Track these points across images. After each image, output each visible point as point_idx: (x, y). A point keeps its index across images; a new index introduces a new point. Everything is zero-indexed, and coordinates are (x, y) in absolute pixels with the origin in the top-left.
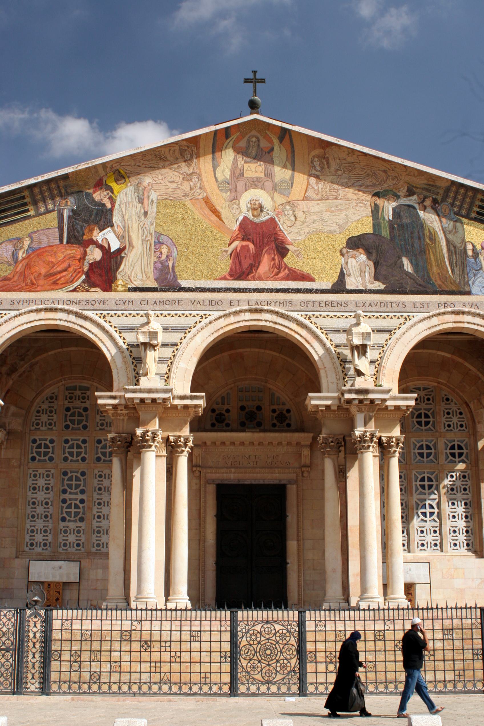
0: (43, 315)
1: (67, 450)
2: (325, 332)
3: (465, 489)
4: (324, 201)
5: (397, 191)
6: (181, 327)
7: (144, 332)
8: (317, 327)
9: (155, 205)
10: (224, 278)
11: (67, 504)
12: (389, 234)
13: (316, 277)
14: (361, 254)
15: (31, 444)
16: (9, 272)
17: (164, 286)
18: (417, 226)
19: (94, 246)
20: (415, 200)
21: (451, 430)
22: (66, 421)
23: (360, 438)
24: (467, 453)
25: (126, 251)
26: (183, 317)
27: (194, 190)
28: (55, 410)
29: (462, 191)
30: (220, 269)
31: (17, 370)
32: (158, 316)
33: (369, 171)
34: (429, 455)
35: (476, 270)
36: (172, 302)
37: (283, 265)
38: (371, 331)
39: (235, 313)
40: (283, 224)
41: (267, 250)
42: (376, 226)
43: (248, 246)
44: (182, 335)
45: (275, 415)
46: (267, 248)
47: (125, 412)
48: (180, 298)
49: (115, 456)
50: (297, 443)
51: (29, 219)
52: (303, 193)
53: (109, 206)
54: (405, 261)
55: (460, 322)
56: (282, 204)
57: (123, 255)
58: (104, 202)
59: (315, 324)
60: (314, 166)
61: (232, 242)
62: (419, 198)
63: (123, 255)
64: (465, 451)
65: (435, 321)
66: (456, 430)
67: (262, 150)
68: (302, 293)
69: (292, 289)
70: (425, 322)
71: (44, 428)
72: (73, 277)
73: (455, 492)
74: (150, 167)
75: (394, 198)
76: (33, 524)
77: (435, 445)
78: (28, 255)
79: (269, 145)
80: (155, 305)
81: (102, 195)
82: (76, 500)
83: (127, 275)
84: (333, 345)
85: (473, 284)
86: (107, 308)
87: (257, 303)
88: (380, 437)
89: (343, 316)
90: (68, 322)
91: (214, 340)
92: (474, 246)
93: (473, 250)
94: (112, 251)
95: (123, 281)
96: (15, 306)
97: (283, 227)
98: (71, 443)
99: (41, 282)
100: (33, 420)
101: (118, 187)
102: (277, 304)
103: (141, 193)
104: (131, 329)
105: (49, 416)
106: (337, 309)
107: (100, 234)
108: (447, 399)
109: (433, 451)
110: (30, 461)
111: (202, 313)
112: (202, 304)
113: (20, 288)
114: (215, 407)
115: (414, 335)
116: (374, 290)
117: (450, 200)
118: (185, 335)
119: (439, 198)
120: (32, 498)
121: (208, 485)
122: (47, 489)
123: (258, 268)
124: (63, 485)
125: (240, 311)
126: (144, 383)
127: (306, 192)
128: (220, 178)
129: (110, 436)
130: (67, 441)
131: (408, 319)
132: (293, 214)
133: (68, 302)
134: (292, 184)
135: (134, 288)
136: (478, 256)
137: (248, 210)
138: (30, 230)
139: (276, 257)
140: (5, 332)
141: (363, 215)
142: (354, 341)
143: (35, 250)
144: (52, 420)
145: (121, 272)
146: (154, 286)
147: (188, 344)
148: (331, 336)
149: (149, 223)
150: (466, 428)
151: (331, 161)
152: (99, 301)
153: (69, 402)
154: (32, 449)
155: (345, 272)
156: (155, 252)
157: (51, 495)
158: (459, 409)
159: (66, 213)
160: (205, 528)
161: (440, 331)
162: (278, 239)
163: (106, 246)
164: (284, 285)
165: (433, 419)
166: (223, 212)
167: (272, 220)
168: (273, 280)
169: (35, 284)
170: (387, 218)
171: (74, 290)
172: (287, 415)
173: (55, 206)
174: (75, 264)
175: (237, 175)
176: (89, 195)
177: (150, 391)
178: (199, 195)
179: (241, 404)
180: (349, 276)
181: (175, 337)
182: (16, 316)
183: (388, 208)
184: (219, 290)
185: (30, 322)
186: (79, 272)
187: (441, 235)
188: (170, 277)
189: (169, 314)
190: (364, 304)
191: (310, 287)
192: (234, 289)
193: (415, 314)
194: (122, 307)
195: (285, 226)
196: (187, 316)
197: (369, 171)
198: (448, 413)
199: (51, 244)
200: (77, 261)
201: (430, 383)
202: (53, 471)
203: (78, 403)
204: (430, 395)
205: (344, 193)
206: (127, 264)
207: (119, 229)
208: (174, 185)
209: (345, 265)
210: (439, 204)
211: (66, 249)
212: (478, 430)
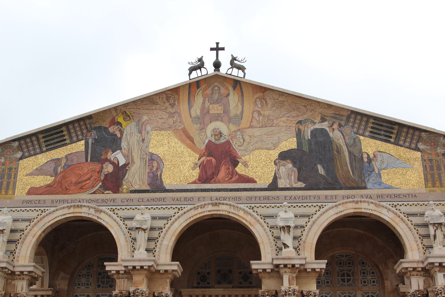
0: (72, 210)
4: (263, 128)
5: (314, 119)
6: (165, 216)
8: (258, 215)
10: (194, 182)
12: (308, 149)
17: (153, 189)
18: (328, 143)
19: (108, 162)
20: (326, 125)
21: (366, 285)
22: (98, 282)
23: (285, 292)
25: (129, 166)
26: (166, 210)
27: (176, 124)
28: (91, 275)
29: (359, 117)
33: (294, 107)
35: (370, 172)
36: (159, 199)
37: (235, 172)
39: (202, 207)
40: (235, 145)
41: (224, 162)
42: (299, 143)
43: (211, 160)
44: (165, 221)
45: (241, 276)
46: (224, 161)
48: (165, 196)
51: (66, 146)
53: (119, 135)
54: (320, 167)
55: (359, 208)
56: (235, 131)
57: (127, 168)
59: (257, 212)
60: (257, 105)
61: (201, 158)
62: (329, 123)
63: (127, 168)
65: (341, 208)
66: (370, 285)
67: (222, 95)
68: (248, 191)
70: (334, 209)
71: (83, 288)
72: (93, 184)
74: (147, 109)
75: (311, 124)
79: (227, 92)
81: (115, 128)
83: (130, 181)
84: (269, 227)
85: (368, 181)
87: (217, 199)
91: (187, 225)
92: (368, 155)
94: (120, 165)
95: (127, 186)
97: (235, 146)
99: (72, 188)
102: (231, 199)
103: (141, 127)
105: (87, 279)
106: (271, 201)
107: (113, 155)
108: (363, 263)
111: (179, 206)
112: (179, 200)
113: (58, 192)
117: (351, 124)
118: (167, 222)
119: (343, 123)
123: (218, 175)
127: (251, 122)
128: (193, 114)
131: (322, 208)
132: (242, 137)
133: (90, 201)
134: (242, 117)
135: (134, 190)
136: (371, 162)
137: (212, 136)
139: (230, 167)
140: (46, 222)
141: (290, 137)
143: (69, 166)
144: (89, 281)
145: (126, 180)
147: (169, 228)
148: (267, 220)
149: (145, 146)
150: (377, 283)
151: (268, 101)
152: (111, 200)
153: (101, 269)
155: (278, 176)
156: (149, 166)
158: (372, 270)
159: (90, 141)
161: (345, 215)
162: (232, 155)
163: (116, 162)
164: (235, 186)
165: (353, 278)
166: (195, 137)
167: (228, 143)
168: (228, 183)
170: (306, 138)
173: (83, 136)
176: (106, 129)
177: (140, 260)
178: (179, 127)
180: (280, 178)
183: (308, 131)
185: (63, 215)
186: (98, 180)
187: (345, 148)
188: (158, 182)
189: (157, 208)
190: (291, 198)
192: (201, 189)
193: (326, 204)
194: (126, 204)
195: (237, 146)
196: (169, 209)
197: (294, 107)
198: (364, 273)
199: (79, 162)
200: (97, 173)
204: (351, 260)
205: (277, 122)
206: (130, 175)
208: (162, 121)
209: (277, 171)
211: (90, 165)
212: (386, 285)
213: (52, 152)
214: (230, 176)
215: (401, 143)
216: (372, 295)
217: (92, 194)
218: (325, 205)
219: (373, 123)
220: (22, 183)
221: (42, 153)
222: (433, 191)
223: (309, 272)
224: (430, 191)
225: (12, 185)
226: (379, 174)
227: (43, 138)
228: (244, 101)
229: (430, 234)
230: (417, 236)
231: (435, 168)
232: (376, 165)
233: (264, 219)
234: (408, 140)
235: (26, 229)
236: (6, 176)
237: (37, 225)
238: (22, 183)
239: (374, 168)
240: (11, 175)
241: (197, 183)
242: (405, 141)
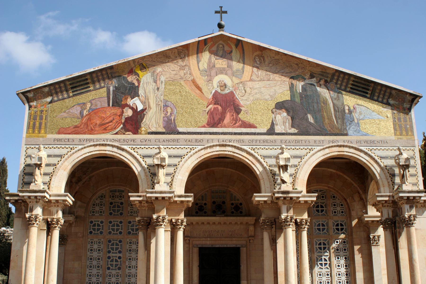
0: (98, 148)
1: (111, 227)
2: (263, 158)
3: (345, 250)
7: (157, 158)
8: (258, 155)
9: (163, 84)
10: (204, 127)
11: (110, 260)
13: (258, 126)
14: (284, 112)
15: (90, 224)
16: (78, 123)
17: (169, 131)
19: (128, 107)
20: (314, 81)
21: (336, 215)
23: (284, 219)
24: (346, 228)
25: (147, 111)
28: (104, 204)
30: (201, 121)
31: (81, 180)
32: (165, 149)
33: (288, 64)
34: (323, 229)
35: (351, 121)
36: (174, 140)
38: (290, 157)
39: (211, 147)
40: (238, 95)
42: (293, 95)
43: (217, 108)
44: (179, 159)
45: (233, 206)
46: (229, 109)
47: (146, 205)
49: (140, 231)
50: (246, 223)
52: (250, 77)
53: (136, 84)
54: (309, 116)
55: (342, 152)
56: (237, 83)
57: (145, 113)
58: (134, 82)
59: (257, 153)
61: (209, 106)
62: (317, 80)
63: (145, 113)
64: (344, 227)
65: (327, 151)
66: (339, 215)
67: (226, 52)
69: (244, 133)
70: (321, 152)
72: (115, 126)
73: (339, 251)
76: (91, 271)
77: (327, 224)
78: (89, 113)
79: (230, 49)
80: (164, 142)
81: (132, 78)
82: (116, 257)
83: (147, 124)
85: (349, 129)
86: (136, 144)
87: (223, 141)
88: (296, 219)
89: (273, 148)
90: (112, 152)
93: (349, 110)
94: (138, 110)
96: (82, 143)
98: (113, 223)
99: (97, 129)
100: (91, 210)
101: (142, 73)
102: (235, 141)
103: (155, 77)
104: (149, 156)
105: (100, 207)
107: (132, 101)
108: (334, 197)
109: (326, 227)
110: (89, 234)
111: (191, 147)
112: (191, 142)
113: (84, 132)
114: (198, 202)
115: (315, 159)
116: (291, 133)
117: (335, 81)
119: (329, 80)
120: (90, 256)
121: (194, 248)
122: (99, 250)
123: (223, 121)
124: (108, 248)
125: (213, 146)
126: (157, 188)
127: (251, 77)
128: (201, 68)
129: (137, 219)
130: (110, 222)
131: (311, 150)
133: (113, 141)
134: (243, 71)
136: (352, 113)
137: (218, 87)
138: (91, 98)
139: (234, 114)
140: (76, 158)
142: (280, 163)
145: (144, 123)
146: (163, 131)
148: (266, 160)
149: (160, 94)
150: (345, 213)
151: (266, 58)
152: (131, 140)
153: (112, 199)
154: (90, 227)
155: (274, 123)
156: (163, 111)
157: (101, 254)
158: (341, 202)
159: (111, 89)
160: (192, 273)
161: (330, 157)
163: (135, 108)
164: (239, 130)
167: (232, 93)
169: (93, 130)
170: (298, 91)
171: (116, 134)
172: (240, 206)
173: (105, 84)
174: (117, 119)
175: (211, 66)
176: (124, 78)
177: (161, 192)
178: (189, 78)
179: (213, 200)
180: (277, 125)
181: (175, 161)
182: (82, 149)
183: (299, 85)
184: (201, 133)
185: (90, 152)
186: (119, 123)
187: (330, 101)
188: (172, 126)
189: (172, 148)
191: (254, 132)
194: (144, 143)
195: (239, 96)
196: (182, 149)
198: (335, 205)
200: (118, 117)
201: (324, 187)
202: (102, 240)
203: (117, 200)
204: (324, 194)
205: (273, 77)
206: (147, 118)
207: (143, 98)
208: (174, 72)
210: (329, 83)
211: (112, 110)
212: (352, 215)
213: (78, 97)
214: (234, 122)
215: (376, 98)
216: (341, 223)
217: (114, 134)
218: (314, 148)
219: (353, 81)
220: (52, 124)
221: (69, 98)
222: (400, 139)
223: (302, 203)
224: (398, 138)
225: (44, 126)
226: (358, 124)
227: (70, 84)
228: (245, 58)
229: (395, 174)
230: (388, 175)
231: (402, 120)
232: (356, 115)
233: (264, 159)
234: (381, 96)
235: (58, 164)
236: (38, 117)
237: (67, 160)
238: (52, 124)
239: (353, 118)
240: (42, 116)
241: (206, 127)
242: (378, 97)
